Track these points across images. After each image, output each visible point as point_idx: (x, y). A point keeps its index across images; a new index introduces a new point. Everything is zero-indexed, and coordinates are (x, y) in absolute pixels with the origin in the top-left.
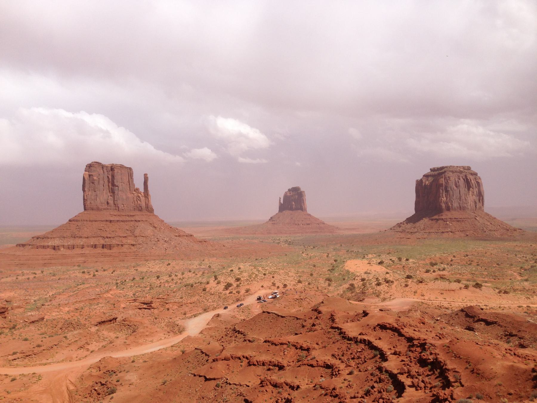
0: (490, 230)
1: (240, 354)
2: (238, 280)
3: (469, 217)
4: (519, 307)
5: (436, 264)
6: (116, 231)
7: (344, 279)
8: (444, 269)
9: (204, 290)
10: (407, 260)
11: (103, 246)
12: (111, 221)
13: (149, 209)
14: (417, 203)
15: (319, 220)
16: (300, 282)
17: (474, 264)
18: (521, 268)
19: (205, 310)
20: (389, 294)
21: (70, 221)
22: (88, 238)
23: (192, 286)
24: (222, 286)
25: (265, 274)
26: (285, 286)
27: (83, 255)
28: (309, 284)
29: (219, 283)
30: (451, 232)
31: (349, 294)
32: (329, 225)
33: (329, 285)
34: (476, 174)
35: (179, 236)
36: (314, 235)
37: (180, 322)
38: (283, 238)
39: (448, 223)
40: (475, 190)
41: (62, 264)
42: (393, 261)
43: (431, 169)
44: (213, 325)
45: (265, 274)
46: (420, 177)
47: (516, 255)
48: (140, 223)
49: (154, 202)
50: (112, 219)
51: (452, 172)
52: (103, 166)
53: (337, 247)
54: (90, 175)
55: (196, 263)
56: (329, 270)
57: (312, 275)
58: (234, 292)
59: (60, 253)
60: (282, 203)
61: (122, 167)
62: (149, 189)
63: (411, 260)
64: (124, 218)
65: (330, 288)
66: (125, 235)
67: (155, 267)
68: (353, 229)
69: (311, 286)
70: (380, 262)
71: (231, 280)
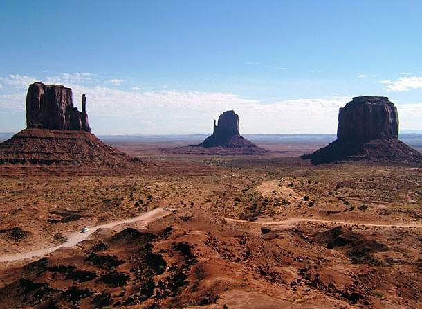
0: (403, 157)
1: (67, 264)
2: (150, 197)
4: (393, 227)
5: (342, 187)
6: (55, 148)
7: (251, 200)
8: (346, 192)
9: (118, 205)
10: (316, 183)
11: (42, 162)
12: (50, 138)
13: (88, 129)
16: (208, 201)
17: (377, 187)
18: (416, 192)
19: (97, 224)
20: (282, 214)
21: (16, 137)
22: (28, 153)
23: (109, 201)
25: (177, 193)
26: (192, 204)
27: (23, 169)
28: (217, 203)
29: (132, 199)
31: (250, 214)
33: (235, 205)
34: (392, 104)
35: (113, 154)
36: (244, 156)
37: (64, 235)
38: (215, 158)
40: (390, 119)
41: (4, 176)
42: (303, 184)
44: (93, 238)
45: (177, 193)
46: (343, 105)
47: (416, 180)
49: (90, 122)
50: (52, 136)
52: (44, 86)
53: (261, 169)
55: (123, 180)
56: (242, 191)
57: (224, 195)
58: (143, 208)
59: (3, 166)
61: (62, 87)
62: (87, 108)
63: (319, 183)
64: (62, 136)
65: (236, 208)
67: (87, 182)
68: (284, 152)
69: (218, 205)
71: (144, 198)
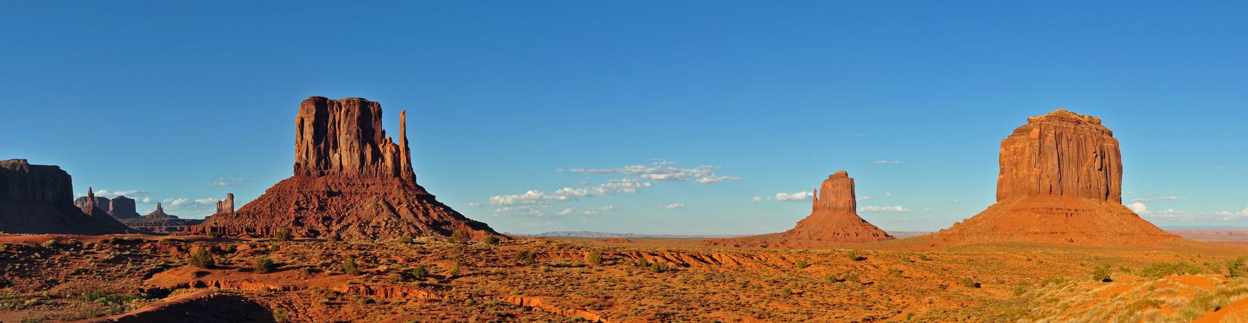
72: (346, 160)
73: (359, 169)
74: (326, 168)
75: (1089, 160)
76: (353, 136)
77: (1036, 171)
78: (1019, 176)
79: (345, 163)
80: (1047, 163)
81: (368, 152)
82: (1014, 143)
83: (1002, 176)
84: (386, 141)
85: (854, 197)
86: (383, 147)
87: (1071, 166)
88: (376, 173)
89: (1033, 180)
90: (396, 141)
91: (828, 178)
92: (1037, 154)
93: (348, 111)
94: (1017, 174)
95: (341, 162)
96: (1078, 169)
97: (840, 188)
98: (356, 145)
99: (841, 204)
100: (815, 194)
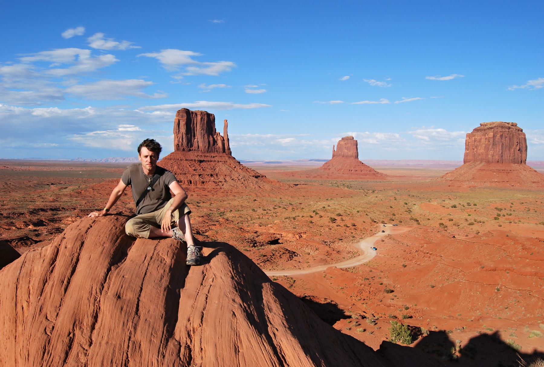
0: (533, 182)
3: (514, 169)
8: (510, 215)
14: (466, 155)
15: (369, 167)
24: (325, 221)
30: (498, 182)
32: (378, 172)
39: (495, 173)
43: (480, 124)
48: (220, 163)
51: (502, 127)
54: (179, 120)
60: (336, 150)
66: (208, 173)
70: (454, 206)
72: (201, 143)
73: (208, 148)
74: (191, 147)
75: (514, 146)
76: (204, 131)
77: (491, 152)
78: (478, 152)
79: (201, 145)
80: (497, 148)
81: (211, 139)
82: (474, 136)
83: (468, 151)
84: (217, 134)
85: (357, 150)
86: (216, 137)
87: (507, 150)
88: (215, 150)
89: (490, 156)
90: (222, 134)
91: (341, 139)
92: (492, 145)
93: (202, 118)
94: (476, 151)
95: (198, 145)
96: (509, 150)
97: (349, 145)
98: (206, 136)
99: (350, 153)
100: (334, 148)
